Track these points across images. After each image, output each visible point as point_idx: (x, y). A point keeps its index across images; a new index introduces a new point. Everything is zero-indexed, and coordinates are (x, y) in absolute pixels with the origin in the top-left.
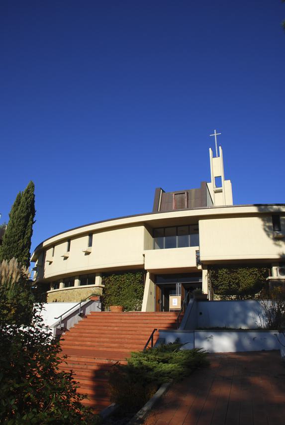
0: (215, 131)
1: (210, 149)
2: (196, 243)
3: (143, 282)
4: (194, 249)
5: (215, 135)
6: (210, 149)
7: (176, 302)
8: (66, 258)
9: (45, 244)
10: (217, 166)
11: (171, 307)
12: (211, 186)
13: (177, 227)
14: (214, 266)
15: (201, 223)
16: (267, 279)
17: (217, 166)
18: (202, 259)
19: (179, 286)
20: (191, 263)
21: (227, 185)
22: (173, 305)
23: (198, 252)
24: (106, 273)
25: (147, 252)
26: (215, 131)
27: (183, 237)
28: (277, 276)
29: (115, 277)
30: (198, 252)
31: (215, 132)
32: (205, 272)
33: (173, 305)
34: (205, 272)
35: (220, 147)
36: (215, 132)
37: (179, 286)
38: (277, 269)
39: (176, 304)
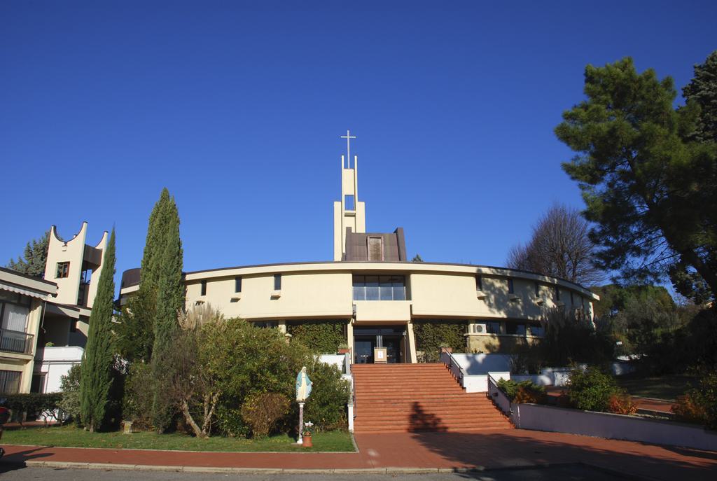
0: (348, 131)
1: (343, 157)
2: (409, 298)
3: (344, 333)
4: (408, 303)
5: (348, 137)
6: (343, 157)
7: (382, 355)
8: (235, 300)
9: (188, 278)
10: (349, 181)
11: (376, 360)
12: (338, 207)
13: (379, 276)
14: (417, 320)
15: (413, 276)
16: (465, 335)
17: (349, 181)
18: (414, 313)
19: (379, 338)
20: (406, 317)
21: (360, 207)
22: (379, 357)
23: (411, 306)
24: (292, 323)
25: (356, 302)
26: (348, 131)
27: (385, 289)
28: (474, 332)
29: (308, 327)
30: (411, 306)
31: (348, 134)
32: (410, 326)
33: (379, 357)
34: (410, 326)
35: (356, 157)
36: (348, 134)
37: (379, 338)
38: (474, 326)
39: (382, 357)
